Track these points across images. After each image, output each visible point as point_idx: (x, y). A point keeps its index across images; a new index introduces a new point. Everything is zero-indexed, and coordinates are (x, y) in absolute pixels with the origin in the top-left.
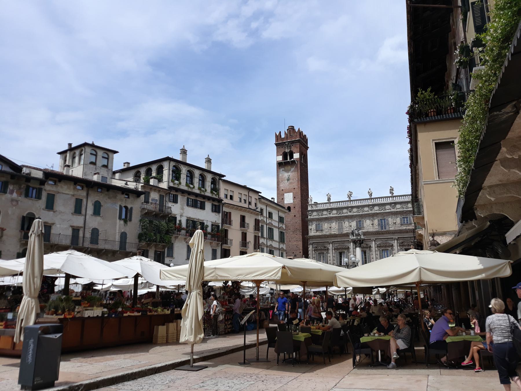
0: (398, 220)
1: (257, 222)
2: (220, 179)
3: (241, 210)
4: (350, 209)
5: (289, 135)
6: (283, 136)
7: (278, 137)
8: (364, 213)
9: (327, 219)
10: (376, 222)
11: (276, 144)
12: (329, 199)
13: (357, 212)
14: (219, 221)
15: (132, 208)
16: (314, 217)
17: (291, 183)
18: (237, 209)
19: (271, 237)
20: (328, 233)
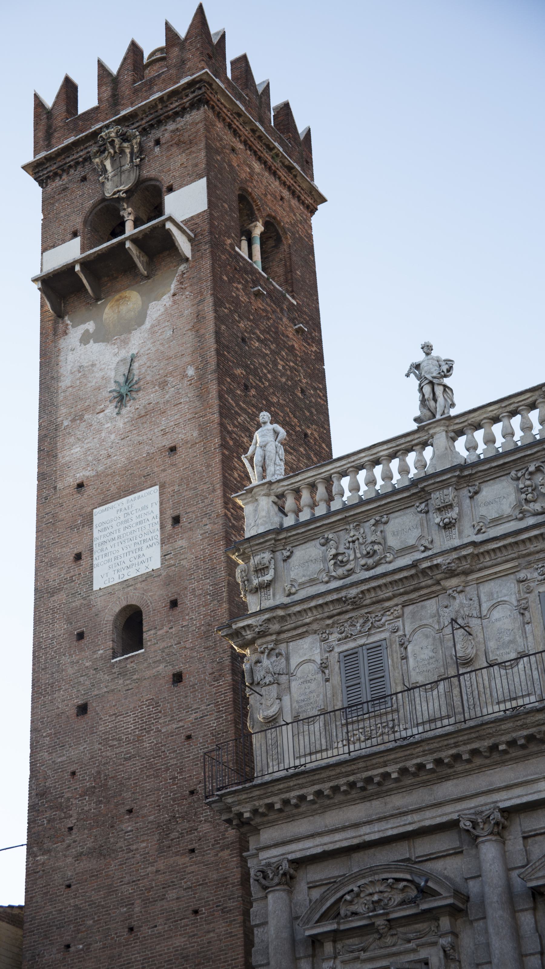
6: (88, 99)
9: (423, 580)
11: (35, 169)
17: (144, 416)
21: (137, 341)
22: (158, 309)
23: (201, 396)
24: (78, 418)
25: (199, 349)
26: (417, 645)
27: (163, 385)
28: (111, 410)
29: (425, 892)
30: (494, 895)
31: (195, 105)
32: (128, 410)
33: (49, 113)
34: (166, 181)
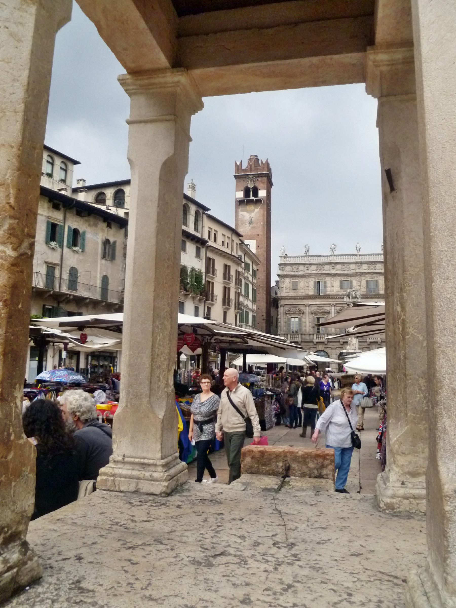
0: (337, 284)
1: (238, 273)
2: (204, 213)
3: (224, 256)
4: (333, 265)
5: (253, 166)
7: (238, 168)
8: (349, 272)
9: (303, 276)
10: (364, 283)
11: (235, 176)
12: (307, 251)
13: (342, 269)
14: (203, 270)
15: (115, 242)
16: (288, 273)
17: (253, 228)
18: (220, 255)
19: (246, 296)
20: (304, 294)
21: (253, 215)
22: (257, 210)
23: (264, 228)
24: (242, 224)
25: (264, 220)
26: (302, 283)
27: (257, 223)
28: (248, 225)
29: (300, 311)
30: (307, 313)
31: (265, 176)
32: (251, 226)
33: (238, 166)
34: (259, 187)
